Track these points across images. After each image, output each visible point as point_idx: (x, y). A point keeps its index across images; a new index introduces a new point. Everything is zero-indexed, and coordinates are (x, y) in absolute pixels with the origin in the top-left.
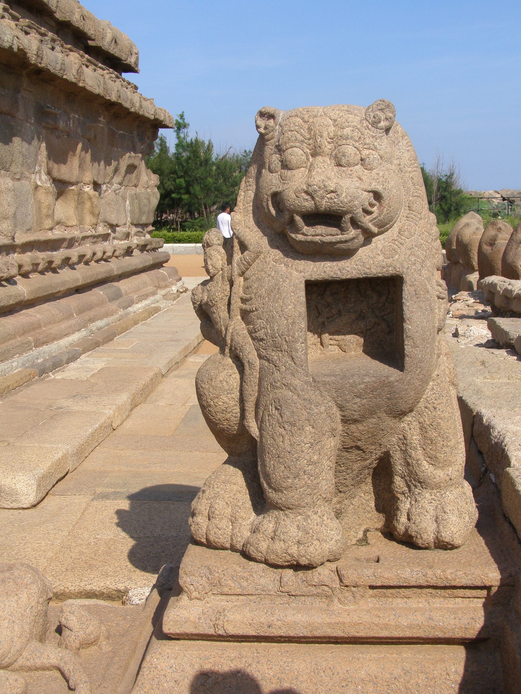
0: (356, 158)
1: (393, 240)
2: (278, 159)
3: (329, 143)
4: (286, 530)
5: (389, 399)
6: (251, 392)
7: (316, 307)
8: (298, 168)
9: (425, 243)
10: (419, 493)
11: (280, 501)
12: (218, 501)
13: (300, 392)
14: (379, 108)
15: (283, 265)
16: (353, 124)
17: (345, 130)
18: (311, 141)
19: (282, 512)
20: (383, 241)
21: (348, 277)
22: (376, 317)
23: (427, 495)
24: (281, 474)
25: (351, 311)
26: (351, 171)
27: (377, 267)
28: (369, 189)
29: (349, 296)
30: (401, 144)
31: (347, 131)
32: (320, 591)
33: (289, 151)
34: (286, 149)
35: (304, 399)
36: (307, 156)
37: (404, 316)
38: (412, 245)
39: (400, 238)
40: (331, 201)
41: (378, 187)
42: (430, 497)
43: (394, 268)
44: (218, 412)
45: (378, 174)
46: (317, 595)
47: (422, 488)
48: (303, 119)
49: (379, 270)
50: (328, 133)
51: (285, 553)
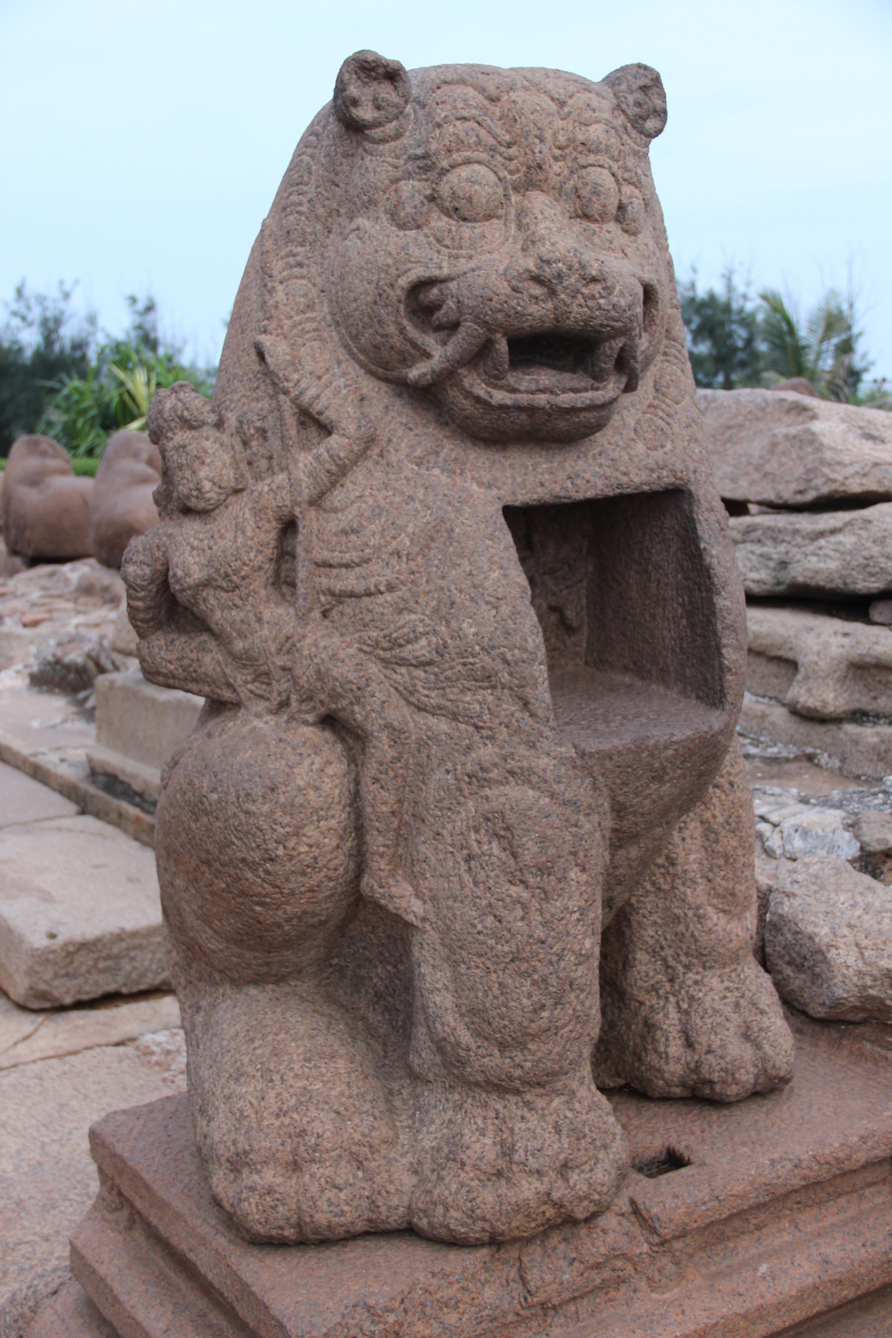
2: (419, 192)
4: (537, 1144)
8: (489, 217)
10: (696, 982)
11: (518, 1072)
12: (313, 1113)
13: (555, 786)
15: (437, 471)
17: (591, 129)
18: (513, 151)
19: (513, 1099)
21: (590, 494)
23: (715, 982)
24: (525, 1001)
27: (639, 469)
31: (596, 132)
32: (606, 1274)
33: (464, 172)
35: (565, 803)
36: (505, 189)
37: (715, 580)
39: (664, 402)
40: (590, 303)
42: (721, 987)
44: (294, 872)
46: (604, 1287)
47: (704, 967)
48: (482, 90)
51: (545, 1203)
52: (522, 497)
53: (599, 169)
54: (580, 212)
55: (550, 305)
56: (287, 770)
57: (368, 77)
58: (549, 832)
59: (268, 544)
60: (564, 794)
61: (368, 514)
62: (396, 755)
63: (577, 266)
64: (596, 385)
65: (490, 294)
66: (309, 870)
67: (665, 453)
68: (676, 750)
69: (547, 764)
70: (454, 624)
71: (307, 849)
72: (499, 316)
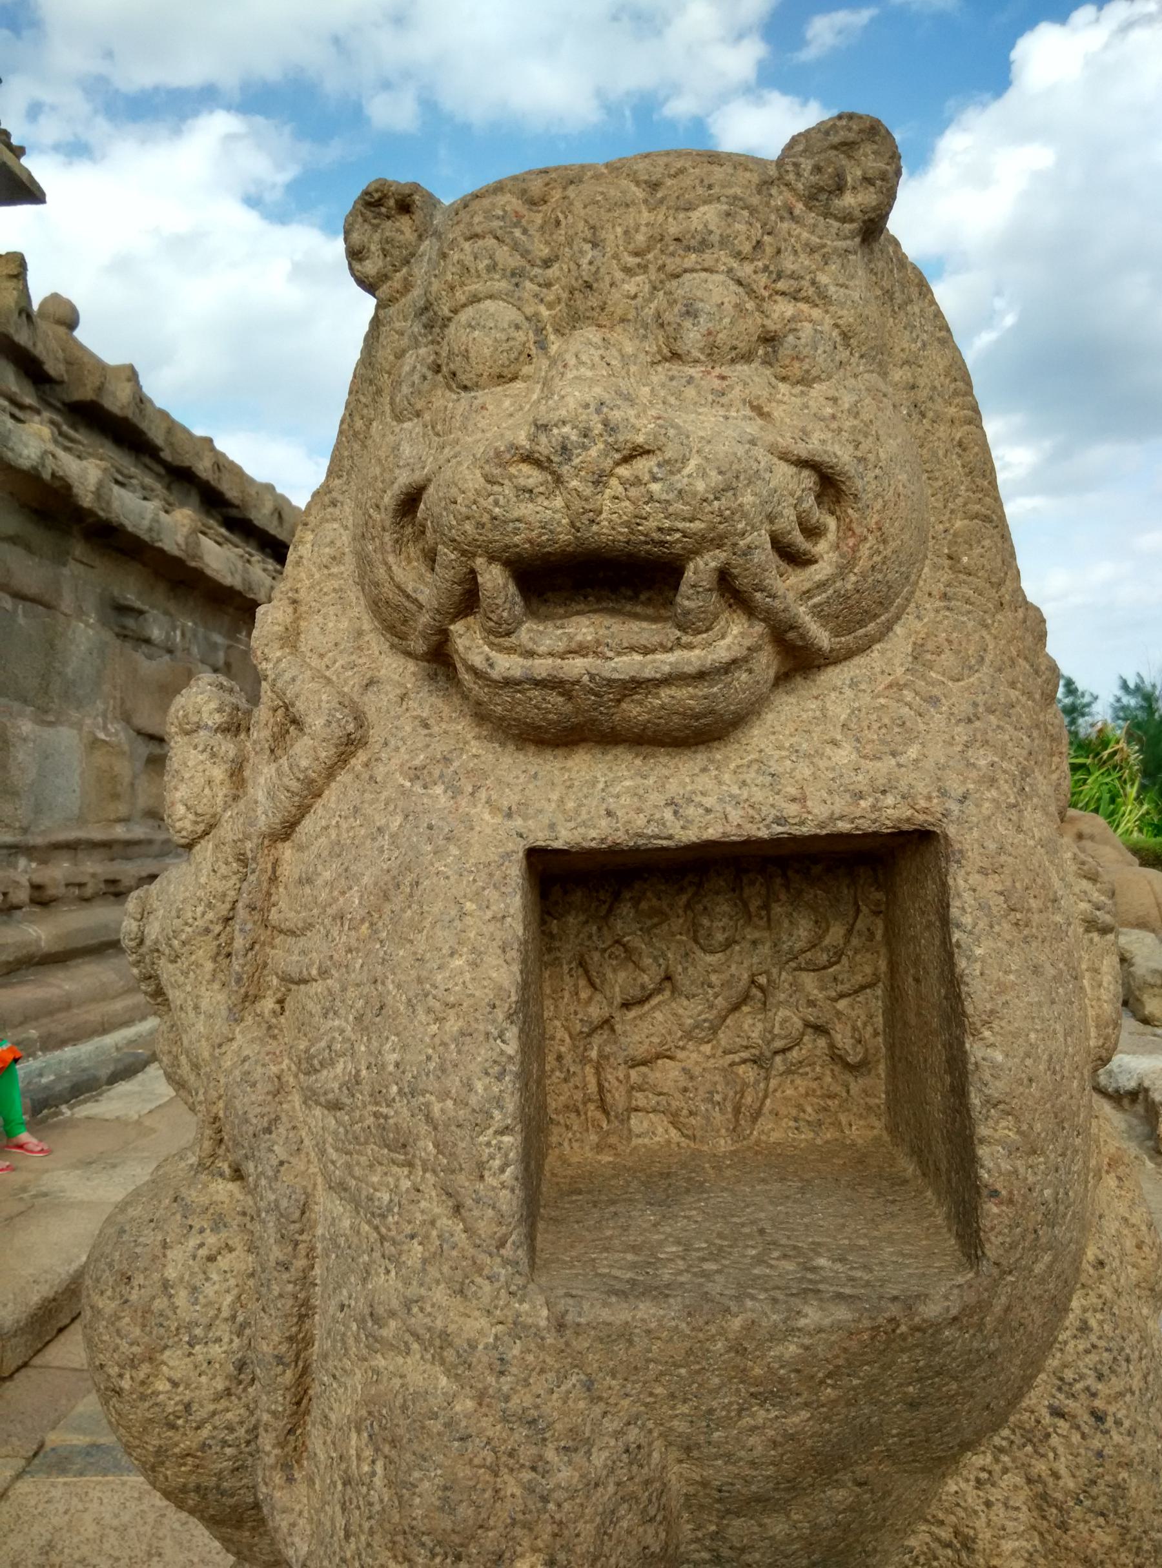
0: (742, 325)
1: (890, 686)
2: (422, 363)
3: (627, 270)
5: (913, 1405)
6: (283, 1348)
7: (582, 964)
9: (1023, 699)
14: (835, 139)
15: (439, 790)
16: (730, 192)
17: (695, 215)
18: (553, 272)
20: (849, 693)
21: (713, 833)
22: (812, 1003)
25: (714, 978)
26: (723, 378)
27: (830, 792)
28: (802, 450)
29: (706, 922)
30: (917, 310)
33: (464, 316)
34: (455, 311)
36: (540, 331)
38: (975, 705)
39: (923, 677)
40: (633, 492)
41: (837, 449)
43: (903, 797)
45: (835, 400)
49: (840, 805)
50: (626, 233)
52: (565, 837)
53: (704, 275)
54: (665, 351)
55: (559, 502)
56: (158, 1251)
57: (379, 215)
58: (463, 1472)
59: (224, 895)
60: (507, 1399)
61: (325, 853)
62: (281, 1258)
63: (598, 428)
64: (685, 639)
65: (454, 491)
66: (180, 1422)
67: (899, 765)
68: (807, 1348)
69: (481, 1332)
70: (375, 1044)
71: (168, 1386)
72: (468, 527)
